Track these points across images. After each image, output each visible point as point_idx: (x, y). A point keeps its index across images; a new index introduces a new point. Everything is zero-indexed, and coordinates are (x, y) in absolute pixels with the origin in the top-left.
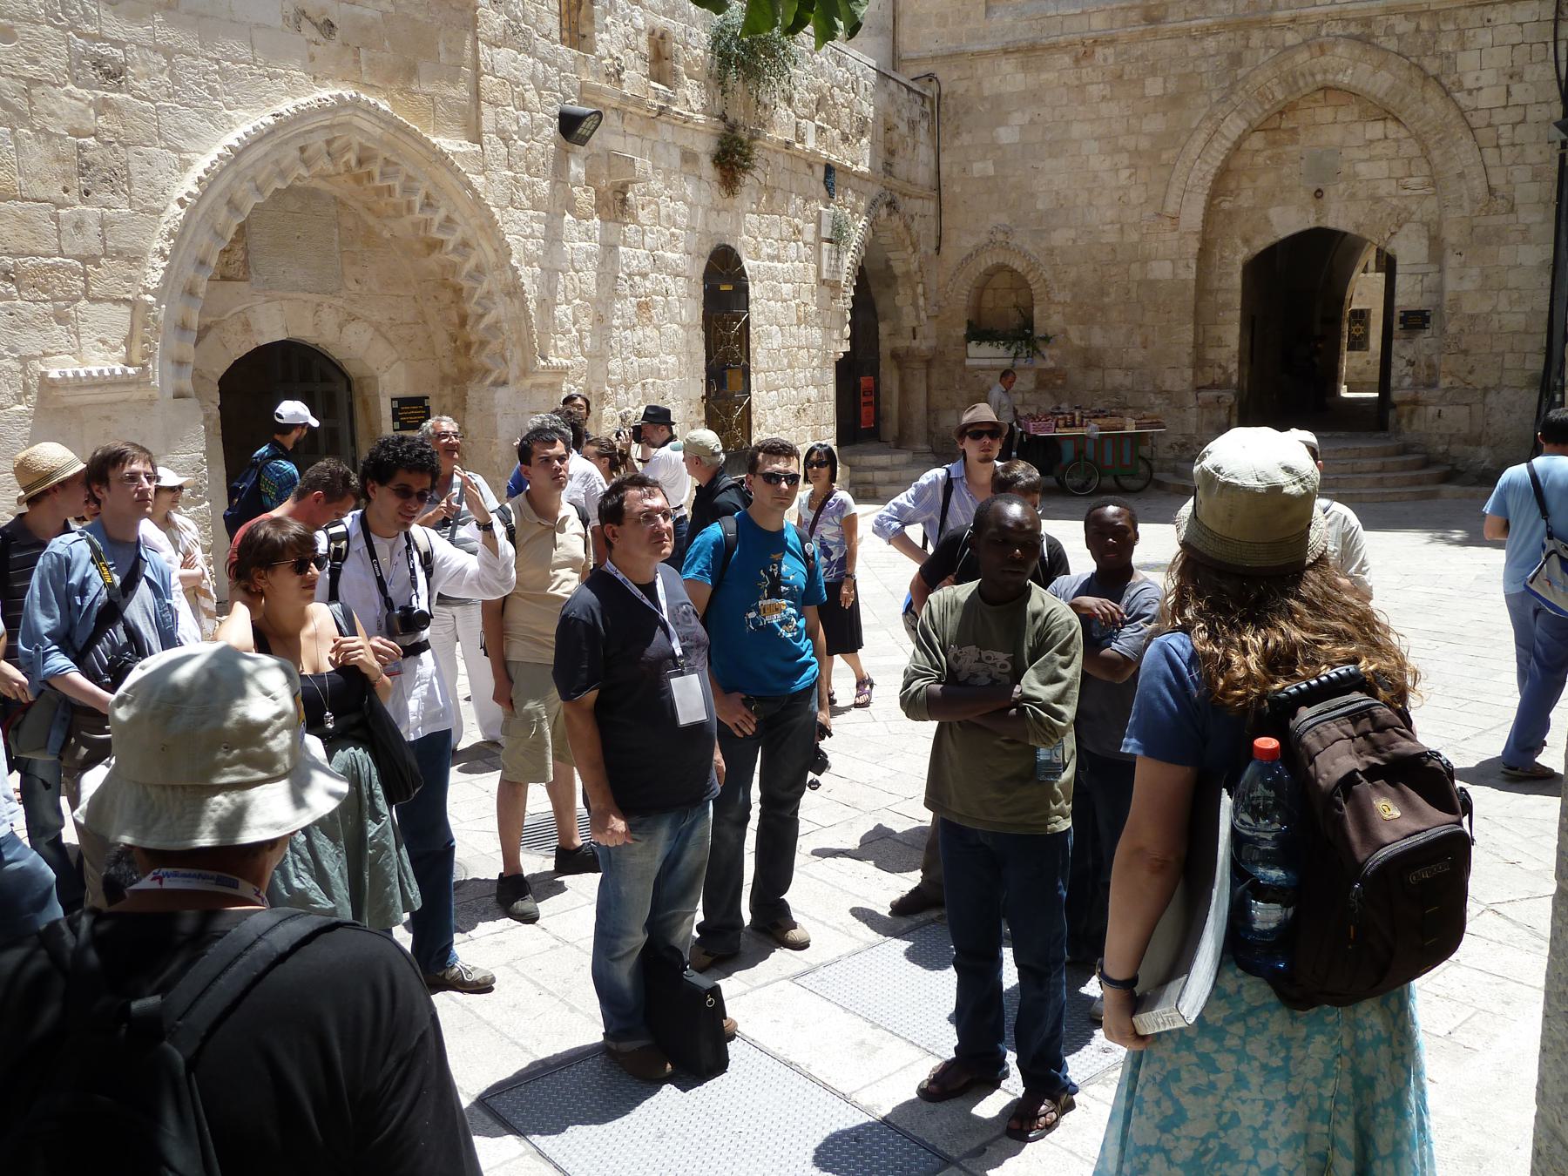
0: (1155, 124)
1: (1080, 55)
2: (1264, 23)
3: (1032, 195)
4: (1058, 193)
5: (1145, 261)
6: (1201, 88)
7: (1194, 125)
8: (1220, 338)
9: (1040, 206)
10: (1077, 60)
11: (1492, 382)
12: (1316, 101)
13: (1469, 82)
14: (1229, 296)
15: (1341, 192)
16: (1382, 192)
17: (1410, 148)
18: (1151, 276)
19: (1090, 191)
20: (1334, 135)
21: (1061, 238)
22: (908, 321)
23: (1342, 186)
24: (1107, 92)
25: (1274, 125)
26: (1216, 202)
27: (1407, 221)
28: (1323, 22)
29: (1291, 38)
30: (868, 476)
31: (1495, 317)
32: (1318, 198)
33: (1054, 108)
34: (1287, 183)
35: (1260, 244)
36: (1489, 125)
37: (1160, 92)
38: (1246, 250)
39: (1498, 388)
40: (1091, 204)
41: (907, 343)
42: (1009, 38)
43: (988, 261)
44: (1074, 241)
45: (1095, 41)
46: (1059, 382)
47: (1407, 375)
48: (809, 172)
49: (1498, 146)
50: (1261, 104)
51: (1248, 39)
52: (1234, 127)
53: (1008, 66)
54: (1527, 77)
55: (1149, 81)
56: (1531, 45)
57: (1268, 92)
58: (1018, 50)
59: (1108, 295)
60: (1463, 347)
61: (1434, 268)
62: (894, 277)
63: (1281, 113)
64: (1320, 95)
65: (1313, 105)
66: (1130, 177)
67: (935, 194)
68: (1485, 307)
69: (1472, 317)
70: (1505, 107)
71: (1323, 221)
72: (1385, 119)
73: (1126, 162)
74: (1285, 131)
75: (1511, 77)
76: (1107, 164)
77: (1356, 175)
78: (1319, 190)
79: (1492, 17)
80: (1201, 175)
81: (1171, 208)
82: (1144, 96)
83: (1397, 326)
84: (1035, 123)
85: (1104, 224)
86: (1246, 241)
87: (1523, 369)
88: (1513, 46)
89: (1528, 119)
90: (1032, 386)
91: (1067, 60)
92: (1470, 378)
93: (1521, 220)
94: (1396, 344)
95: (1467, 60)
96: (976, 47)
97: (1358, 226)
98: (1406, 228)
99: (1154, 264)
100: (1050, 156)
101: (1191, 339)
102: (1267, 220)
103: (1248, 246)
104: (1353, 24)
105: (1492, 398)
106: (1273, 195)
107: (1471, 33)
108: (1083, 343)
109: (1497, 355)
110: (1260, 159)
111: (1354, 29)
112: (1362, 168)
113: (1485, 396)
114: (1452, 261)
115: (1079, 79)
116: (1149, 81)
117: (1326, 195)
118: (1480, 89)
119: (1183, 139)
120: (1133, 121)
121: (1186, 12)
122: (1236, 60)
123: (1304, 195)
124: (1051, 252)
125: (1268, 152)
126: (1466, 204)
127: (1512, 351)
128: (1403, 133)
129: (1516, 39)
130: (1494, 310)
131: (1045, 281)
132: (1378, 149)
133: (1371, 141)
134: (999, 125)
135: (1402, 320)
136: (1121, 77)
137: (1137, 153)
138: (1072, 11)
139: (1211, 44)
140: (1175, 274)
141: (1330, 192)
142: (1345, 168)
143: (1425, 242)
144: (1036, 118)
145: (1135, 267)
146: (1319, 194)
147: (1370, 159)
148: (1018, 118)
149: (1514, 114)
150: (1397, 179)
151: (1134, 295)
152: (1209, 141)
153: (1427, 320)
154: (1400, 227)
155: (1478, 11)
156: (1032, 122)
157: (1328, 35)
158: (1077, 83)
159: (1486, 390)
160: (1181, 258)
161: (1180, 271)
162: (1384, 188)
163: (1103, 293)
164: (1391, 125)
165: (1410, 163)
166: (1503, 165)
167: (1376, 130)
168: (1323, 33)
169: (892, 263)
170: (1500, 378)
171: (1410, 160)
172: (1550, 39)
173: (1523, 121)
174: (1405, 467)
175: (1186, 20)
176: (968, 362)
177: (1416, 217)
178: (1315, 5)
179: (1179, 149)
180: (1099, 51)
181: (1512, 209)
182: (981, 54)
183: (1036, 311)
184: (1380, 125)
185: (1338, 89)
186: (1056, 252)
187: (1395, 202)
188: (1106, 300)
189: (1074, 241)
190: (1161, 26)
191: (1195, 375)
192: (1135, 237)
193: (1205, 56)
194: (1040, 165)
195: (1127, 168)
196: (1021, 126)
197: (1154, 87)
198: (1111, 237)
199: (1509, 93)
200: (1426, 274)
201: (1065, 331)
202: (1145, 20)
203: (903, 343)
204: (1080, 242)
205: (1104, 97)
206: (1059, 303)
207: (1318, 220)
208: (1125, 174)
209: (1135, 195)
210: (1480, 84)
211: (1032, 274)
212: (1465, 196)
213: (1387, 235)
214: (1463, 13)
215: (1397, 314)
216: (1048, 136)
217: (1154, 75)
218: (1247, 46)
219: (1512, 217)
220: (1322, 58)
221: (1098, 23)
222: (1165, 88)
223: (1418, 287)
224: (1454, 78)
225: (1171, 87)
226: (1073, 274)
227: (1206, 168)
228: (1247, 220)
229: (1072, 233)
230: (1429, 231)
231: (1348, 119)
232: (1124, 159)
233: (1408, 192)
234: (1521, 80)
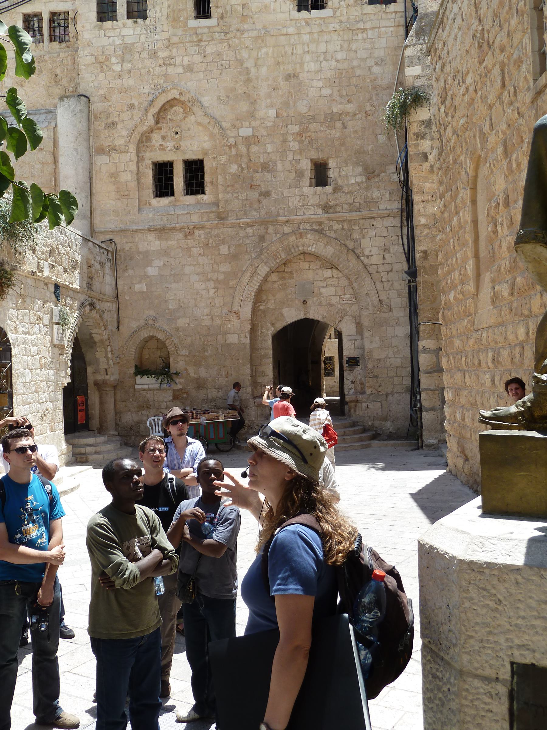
0: (226, 267)
1: (187, 234)
2: (274, 223)
3: (166, 301)
4: (179, 300)
5: (225, 334)
6: (247, 251)
7: (244, 269)
8: (263, 372)
9: (170, 307)
10: (186, 236)
11: (389, 390)
12: (300, 259)
13: (367, 252)
14: (266, 351)
15: (315, 301)
17: (345, 282)
18: (228, 342)
19: (195, 299)
20: (310, 275)
21: (182, 322)
22: (103, 366)
23: (315, 299)
24: (201, 251)
25: (282, 270)
26: (257, 306)
27: (345, 315)
28: (301, 223)
29: (287, 230)
30: (83, 450)
31: (388, 360)
32: (304, 304)
33: (175, 258)
34: (290, 297)
35: (280, 326)
36: (377, 272)
37: (227, 253)
38: (273, 329)
39: (392, 393)
40: (196, 306)
41: (103, 377)
42: (151, 224)
43: (145, 334)
44: (189, 324)
45: (194, 227)
46: (185, 396)
47: (352, 388)
48: (45, 287)
49: (382, 281)
50: (275, 260)
51: (267, 229)
52: (263, 270)
53: (151, 237)
54: (391, 251)
55: (221, 247)
56: (392, 237)
57: (278, 254)
58: (156, 230)
59: (207, 351)
60: (375, 374)
61: (359, 337)
62: (95, 343)
63: (285, 264)
64: (302, 256)
65: (299, 261)
66: (215, 293)
67: (115, 300)
68: (383, 355)
69: (378, 360)
70: (383, 264)
72: (332, 268)
73: (213, 286)
74: (287, 272)
75: (385, 251)
76: (203, 286)
77: (321, 294)
78: (305, 301)
79: (374, 223)
80: (249, 293)
81: (236, 308)
82: (219, 254)
83: (345, 365)
84: (166, 266)
85: (204, 316)
86: (273, 325)
87: (402, 384)
88: (384, 237)
90: (171, 398)
91: (181, 236)
92: (380, 389)
93: (395, 315)
94: (345, 374)
95: (365, 243)
96: (134, 228)
97: (323, 318)
98: (345, 319)
99: (229, 335)
100: (174, 282)
101: (250, 373)
102: (282, 315)
103: (274, 327)
104: (314, 224)
105: (390, 398)
106: (284, 303)
107: (366, 230)
108: (196, 376)
109: (391, 377)
110: (276, 286)
111: (314, 227)
112: (323, 290)
113: (387, 397)
114: (367, 334)
115: (187, 245)
116: (221, 247)
117: (308, 303)
118: (372, 256)
119: (239, 275)
120: (215, 266)
121: (237, 216)
122: (262, 239)
123: (298, 303)
124: (177, 329)
126: (370, 308)
127: (397, 376)
128: (340, 275)
129: (386, 234)
130: (387, 357)
131: (175, 344)
132: (330, 282)
134: (148, 266)
136: (208, 244)
137: (217, 281)
138: (182, 212)
139: (250, 231)
140: (240, 341)
141: (310, 302)
142: (316, 290)
143: (354, 325)
144: (167, 263)
145: (220, 337)
146: (305, 302)
147: (327, 286)
148: (157, 263)
149: (388, 267)
150: (339, 296)
151: (220, 351)
152: (252, 276)
153: (358, 362)
154: (343, 318)
155: (368, 221)
156: (164, 265)
157: (303, 229)
158: (186, 247)
159: (387, 395)
160: (242, 333)
161: (242, 339)
162: (334, 300)
163: (204, 350)
164: (335, 271)
165: (344, 289)
166: (384, 290)
167: (328, 273)
168: (301, 228)
169: (93, 335)
170: (393, 388)
172: (400, 234)
173: (391, 270)
174: (355, 433)
175: (237, 219)
176: (136, 387)
177: (349, 314)
178: (296, 215)
179: (238, 280)
180: (197, 232)
181: (390, 310)
182: (137, 231)
183: (171, 359)
184: (330, 271)
185: (310, 254)
186: (180, 330)
187: (339, 306)
188: (206, 354)
189: (189, 324)
190: (225, 221)
191: (252, 390)
192: (219, 322)
193: (247, 236)
194: (170, 286)
195: (213, 288)
196: (159, 267)
197: (224, 250)
198: (207, 322)
199: (384, 258)
200: (356, 340)
201: (186, 370)
202: (218, 218)
203: (100, 377)
204: (191, 325)
205: (200, 254)
206: (182, 355)
207: (305, 315)
208: (212, 291)
209: (218, 302)
210: (372, 253)
211: (168, 341)
212: (370, 303)
213: (337, 322)
214: (362, 221)
215: (345, 359)
216: (173, 272)
217: (224, 244)
218: (267, 232)
219: (391, 314)
220: (301, 240)
221: (195, 219)
222: (229, 251)
223: (353, 347)
224: (360, 250)
225: (232, 250)
226: (189, 340)
227: (251, 289)
228: (272, 314)
229: (187, 320)
231: (315, 268)
232: (211, 284)
233: (345, 302)
234: (389, 252)
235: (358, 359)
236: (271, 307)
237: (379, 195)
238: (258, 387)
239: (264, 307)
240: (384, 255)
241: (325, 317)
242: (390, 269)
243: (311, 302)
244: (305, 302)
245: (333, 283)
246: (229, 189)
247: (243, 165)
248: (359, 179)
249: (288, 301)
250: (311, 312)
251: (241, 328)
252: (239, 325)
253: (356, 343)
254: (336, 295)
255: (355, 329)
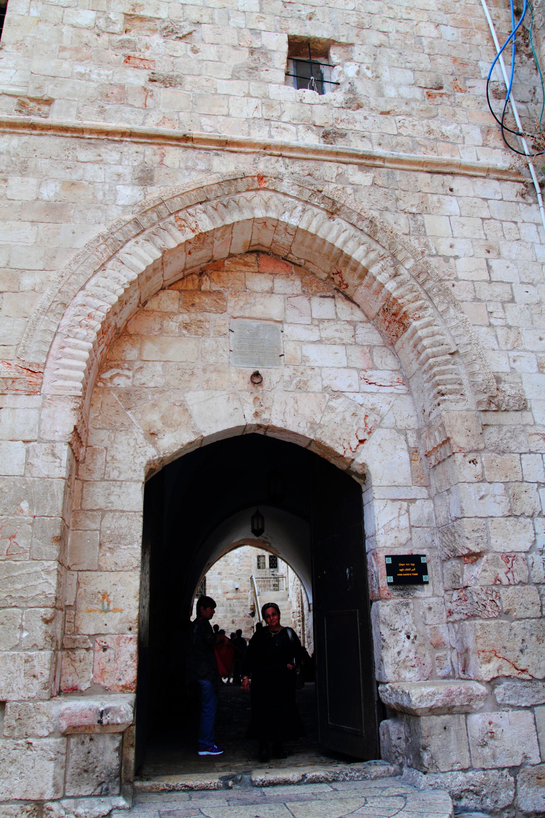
8: (105, 596)
12: (246, 264)
14: (124, 522)
15: (286, 378)
16: (339, 385)
26: (106, 375)
27: (378, 425)
34: (212, 359)
36: (476, 299)
49: (490, 325)
51: (163, 155)
54: (505, 252)
56: (501, 221)
60: (505, 606)
64: (251, 259)
65: (244, 269)
71: (265, 416)
77: (305, 359)
78: (256, 374)
88: (483, 219)
89: (517, 299)
92: (523, 663)
93: (538, 421)
103: (154, 444)
106: (193, 374)
107: (435, 198)
117: (266, 382)
125: (185, 317)
128: (358, 315)
129: (485, 214)
132: (329, 331)
133: (322, 321)
135: (391, 569)
142: (289, 348)
143: (405, 456)
150: (358, 370)
153: (423, 569)
161: (35, 461)
171: (371, 348)
173: (512, 300)
184: (329, 302)
187: (359, 398)
191: (55, 663)
199: (489, 268)
207: (256, 414)
210: (455, 252)
218: (161, 163)
223: (404, 522)
228: (154, 405)
230: (406, 441)
231: (289, 291)
233: (373, 388)
235: (423, 560)
236: (152, 384)
237: (457, 132)
238: (80, 653)
239: (129, 382)
240: (487, 260)
241: (320, 426)
242: (507, 297)
243: (275, 378)
244: (257, 380)
245: (338, 335)
246: (66, 54)
247: (111, 16)
248: (406, 92)
249: (204, 370)
250: (276, 407)
251: (40, 421)
252: (34, 414)
253: (411, 508)
254: (348, 367)
255: (406, 468)
